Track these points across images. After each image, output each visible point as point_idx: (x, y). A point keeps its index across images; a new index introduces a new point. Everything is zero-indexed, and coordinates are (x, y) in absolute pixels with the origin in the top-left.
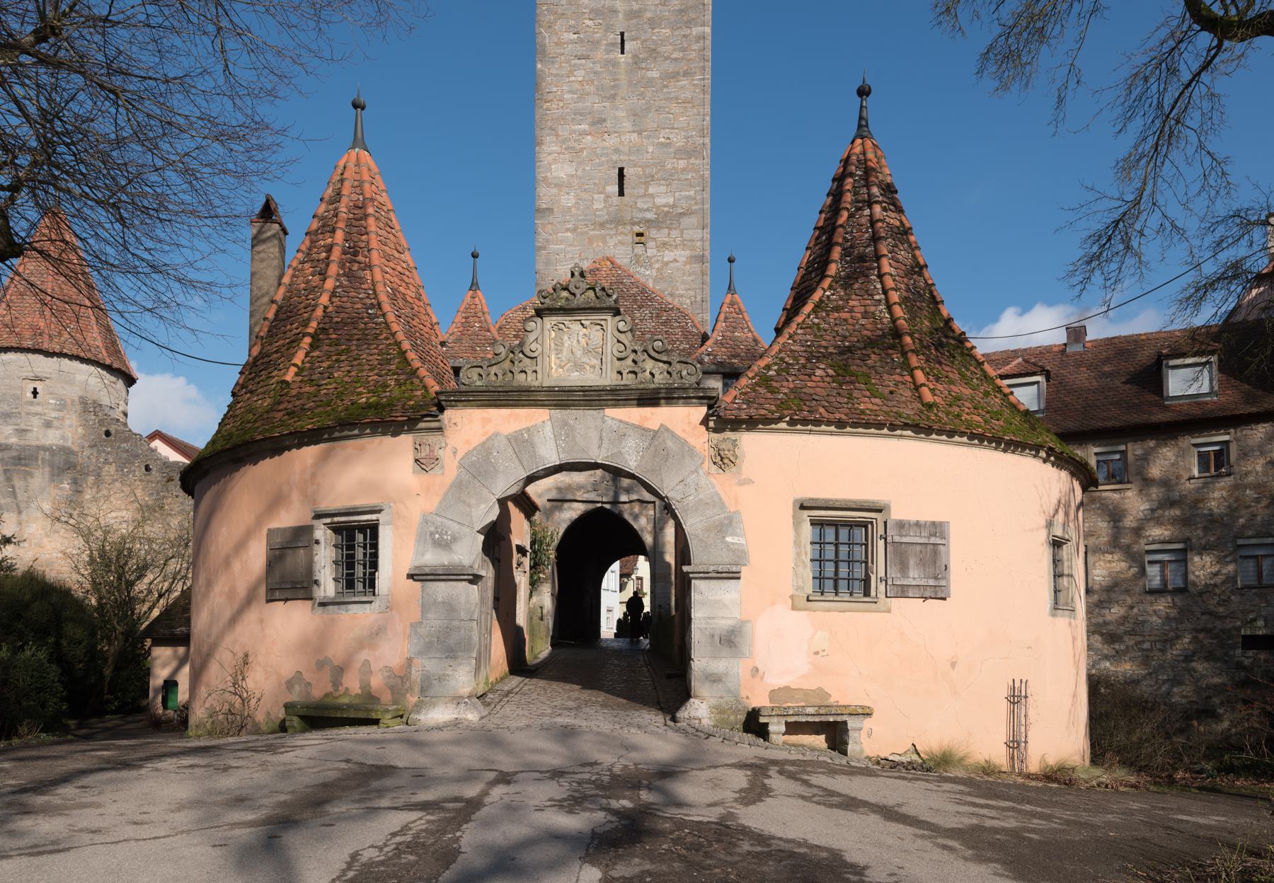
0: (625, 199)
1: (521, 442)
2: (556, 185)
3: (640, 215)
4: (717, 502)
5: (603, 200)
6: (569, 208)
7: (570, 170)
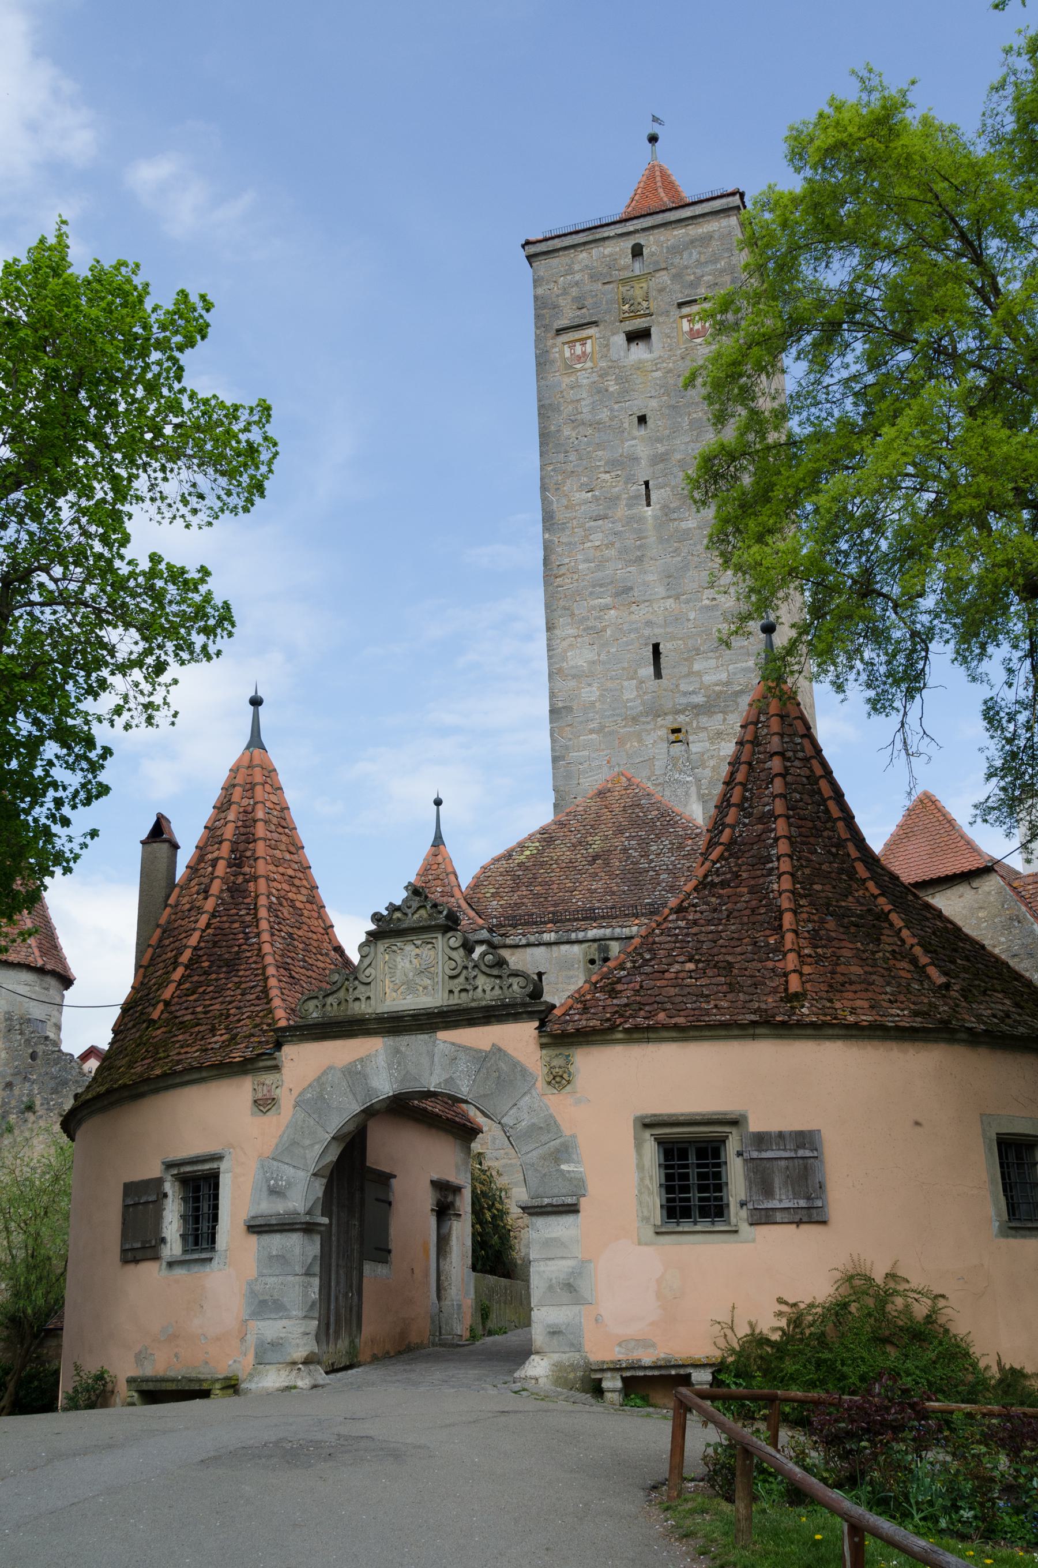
0: (664, 681)
1: (355, 1074)
2: (574, 677)
3: (684, 700)
4: (549, 1126)
5: (635, 686)
6: (593, 703)
7: (589, 655)
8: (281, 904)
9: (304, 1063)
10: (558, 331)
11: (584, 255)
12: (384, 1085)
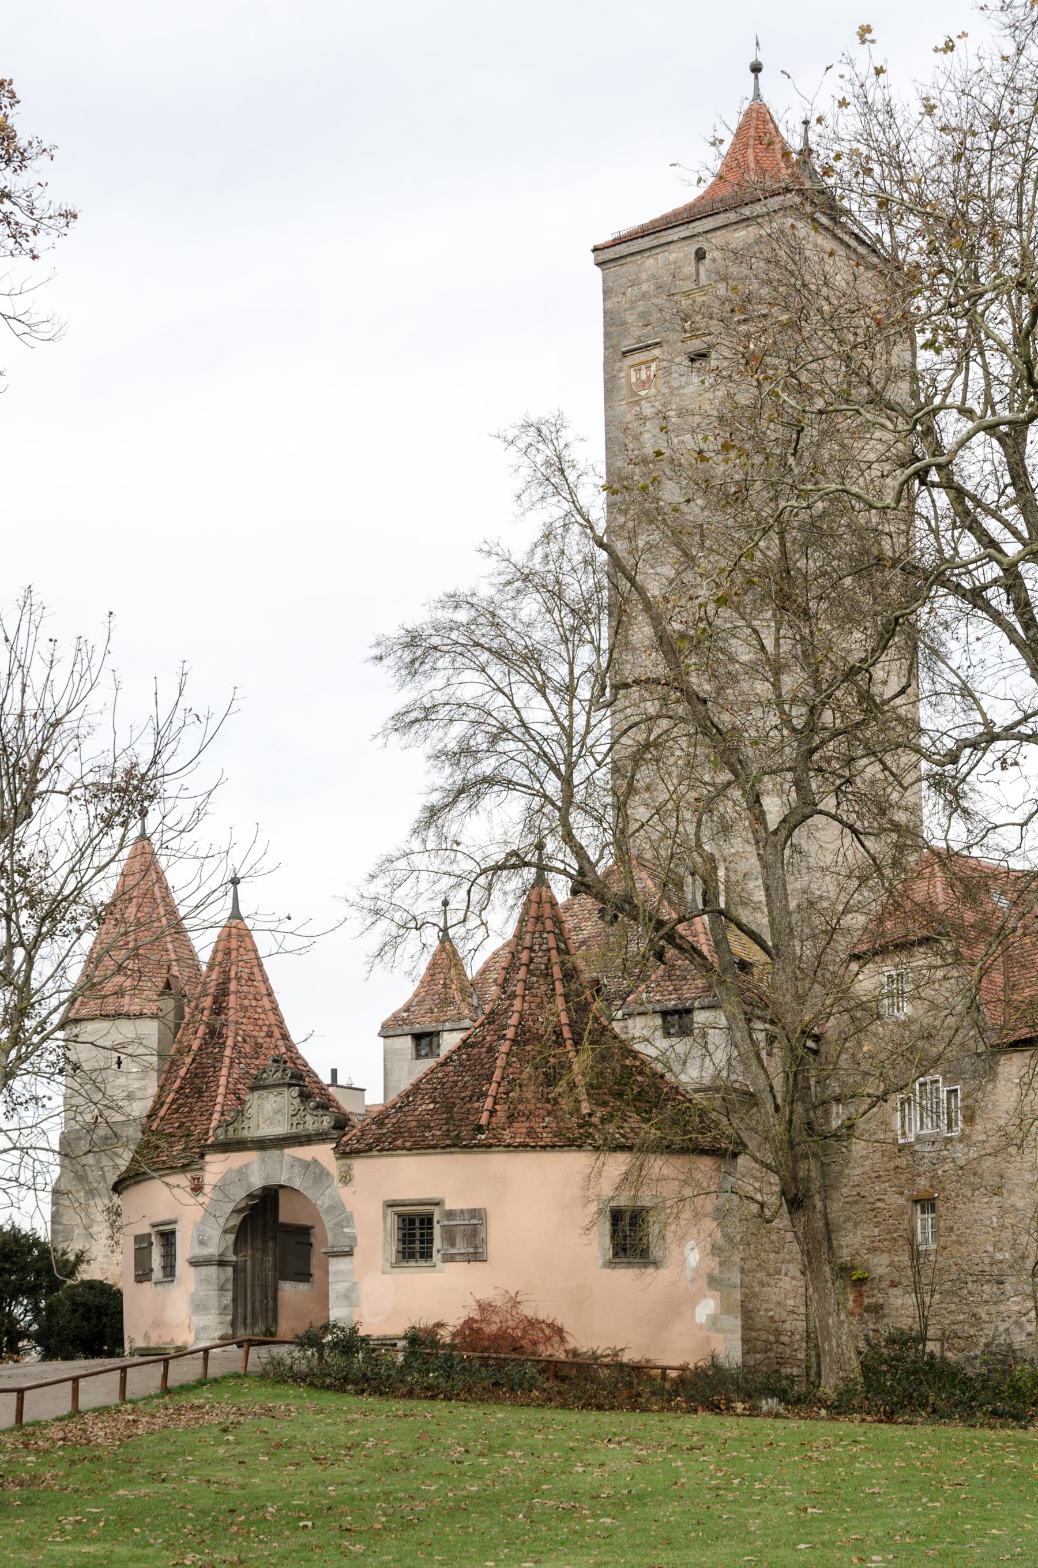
8: (245, 1041)
9: (217, 1167)
10: (624, 353)
11: (651, 261)
12: (257, 1181)
